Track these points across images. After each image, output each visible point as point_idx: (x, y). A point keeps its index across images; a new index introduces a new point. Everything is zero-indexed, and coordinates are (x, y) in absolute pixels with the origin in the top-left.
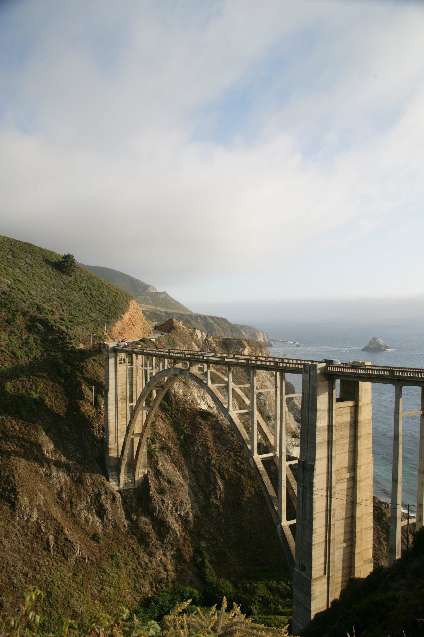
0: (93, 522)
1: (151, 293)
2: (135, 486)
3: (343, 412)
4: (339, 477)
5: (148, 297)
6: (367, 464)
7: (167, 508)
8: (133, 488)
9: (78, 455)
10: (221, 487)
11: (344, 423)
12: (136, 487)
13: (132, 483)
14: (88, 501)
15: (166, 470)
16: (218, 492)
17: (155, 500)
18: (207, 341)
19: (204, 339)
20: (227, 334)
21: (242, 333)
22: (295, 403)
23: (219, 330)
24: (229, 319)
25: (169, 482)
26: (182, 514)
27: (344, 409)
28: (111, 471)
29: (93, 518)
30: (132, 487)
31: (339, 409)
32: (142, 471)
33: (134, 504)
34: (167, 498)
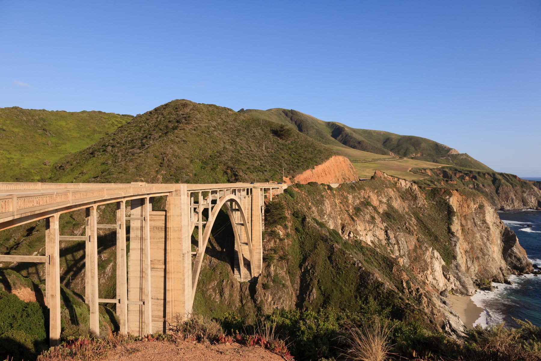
0: (214, 298)
1: (452, 155)
3: (155, 219)
5: (449, 158)
7: (267, 300)
10: (315, 294)
11: (156, 227)
14: (215, 284)
16: (312, 298)
18: (411, 188)
19: (408, 187)
20: (516, 189)
21: (533, 188)
22: (515, 251)
23: (507, 186)
24: (519, 176)
26: (279, 308)
27: (156, 216)
34: (268, 293)
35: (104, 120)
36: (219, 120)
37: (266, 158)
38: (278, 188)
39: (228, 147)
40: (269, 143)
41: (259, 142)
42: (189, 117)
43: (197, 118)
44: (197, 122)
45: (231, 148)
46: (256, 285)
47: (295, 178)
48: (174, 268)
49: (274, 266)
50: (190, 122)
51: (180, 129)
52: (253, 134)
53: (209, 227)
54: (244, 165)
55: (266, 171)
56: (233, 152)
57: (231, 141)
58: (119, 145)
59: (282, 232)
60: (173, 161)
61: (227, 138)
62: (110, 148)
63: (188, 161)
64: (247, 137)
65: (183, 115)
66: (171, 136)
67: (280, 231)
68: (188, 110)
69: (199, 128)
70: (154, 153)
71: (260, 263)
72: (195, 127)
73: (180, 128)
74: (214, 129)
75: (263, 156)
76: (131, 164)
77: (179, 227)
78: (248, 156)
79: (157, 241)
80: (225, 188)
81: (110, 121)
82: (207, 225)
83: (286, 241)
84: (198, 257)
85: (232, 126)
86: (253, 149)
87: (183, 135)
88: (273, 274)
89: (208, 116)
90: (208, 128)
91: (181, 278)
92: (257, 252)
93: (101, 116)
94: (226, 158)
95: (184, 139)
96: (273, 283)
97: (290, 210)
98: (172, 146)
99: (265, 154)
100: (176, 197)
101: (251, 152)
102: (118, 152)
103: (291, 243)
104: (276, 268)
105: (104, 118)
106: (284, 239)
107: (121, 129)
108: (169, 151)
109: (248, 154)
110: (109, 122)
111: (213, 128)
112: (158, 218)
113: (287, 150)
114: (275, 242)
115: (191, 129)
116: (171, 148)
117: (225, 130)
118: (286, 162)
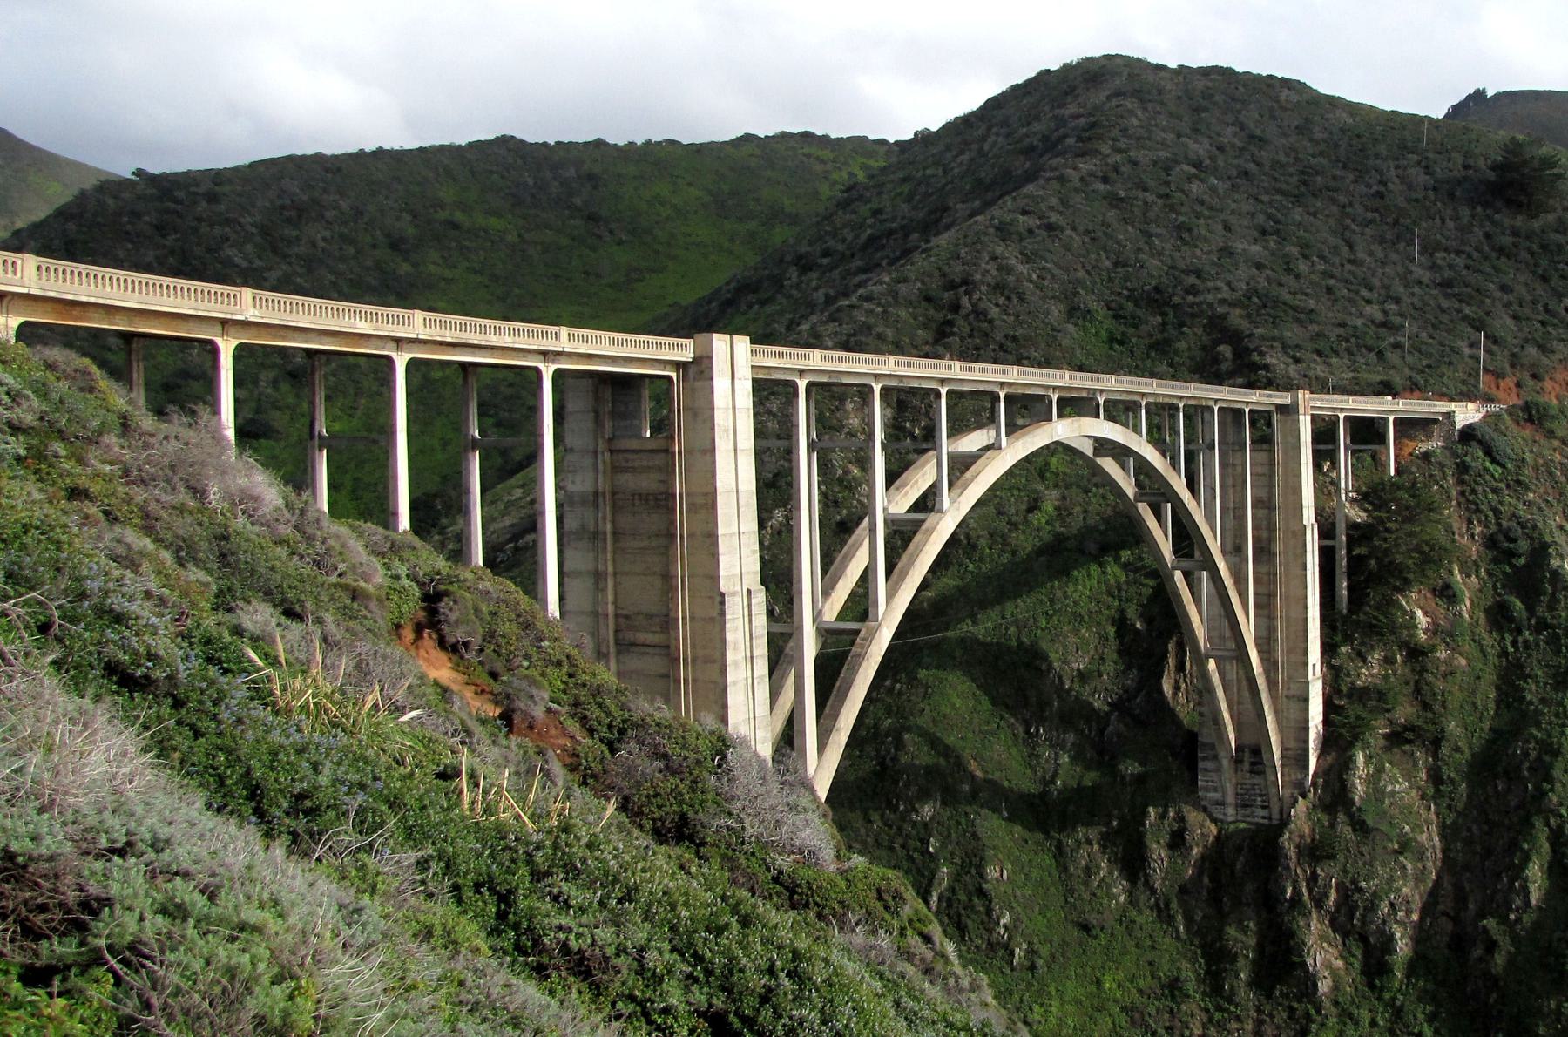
0: (1103, 880)
2: (1270, 819)
3: (636, 464)
4: (630, 636)
6: (704, 619)
8: (1266, 821)
9: (1138, 699)
11: (640, 495)
12: (1275, 822)
13: (1264, 807)
15: (1377, 793)
17: (1288, 867)
25: (1360, 826)
28: (1205, 758)
29: (1110, 873)
30: (1261, 821)
31: (626, 455)
32: (1293, 777)
33: (1239, 866)
35: (818, 168)
36: (1230, 130)
37: (1416, 290)
38: (1435, 421)
39: (1239, 246)
40: (1450, 224)
41: (1396, 222)
42: (1093, 125)
43: (1126, 130)
44: (1122, 144)
45: (1256, 248)
46: (1281, 835)
47: (1548, 385)
48: (693, 646)
49: (1368, 759)
50: (1095, 145)
51: (1049, 179)
52: (1375, 188)
53: (930, 531)
54: (1298, 321)
55: (1397, 346)
56: (1259, 266)
57: (1261, 218)
58: (825, 261)
59: (1426, 614)
60: (994, 312)
61: (1246, 207)
62: (793, 274)
63: (1056, 311)
64: (1343, 199)
65: (1077, 117)
66: (1004, 211)
67: (1419, 613)
68: (1098, 97)
69: (1125, 169)
70: (923, 282)
71: (1307, 742)
72: (1107, 164)
73: (1048, 175)
74: (1193, 171)
75: (1406, 286)
76: (832, 327)
77: (706, 494)
78: (1332, 282)
79: (642, 545)
80: (1047, 387)
81: (840, 169)
82: (924, 527)
83: (1442, 654)
84: (863, 639)
85: (1282, 158)
86: (1361, 255)
87: (1054, 201)
88: (1359, 790)
89: (1179, 118)
90: (1167, 170)
91: (715, 683)
92: (1292, 692)
93: (806, 151)
94: (1225, 293)
95: (1054, 218)
96: (1354, 830)
97: (1479, 522)
98: (999, 250)
99: (1418, 272)
100: (698, 384)
101: (1348, 267)
102: (816, 289)
103: (1463, 662)
104: (1380, 770)
105: (817, 158)
106: (1434, 648)
107: (852, 195)
108: (985, 272)
109: (1332, 277)
110: (835, 176)
111: (1186, 168)
112: (645, 463)
113: (1532, 254)
114: (1388, 661)
115: (1091, 174)
116: (994, 258)
117: (1246, 173)
118: (1516, 307)
